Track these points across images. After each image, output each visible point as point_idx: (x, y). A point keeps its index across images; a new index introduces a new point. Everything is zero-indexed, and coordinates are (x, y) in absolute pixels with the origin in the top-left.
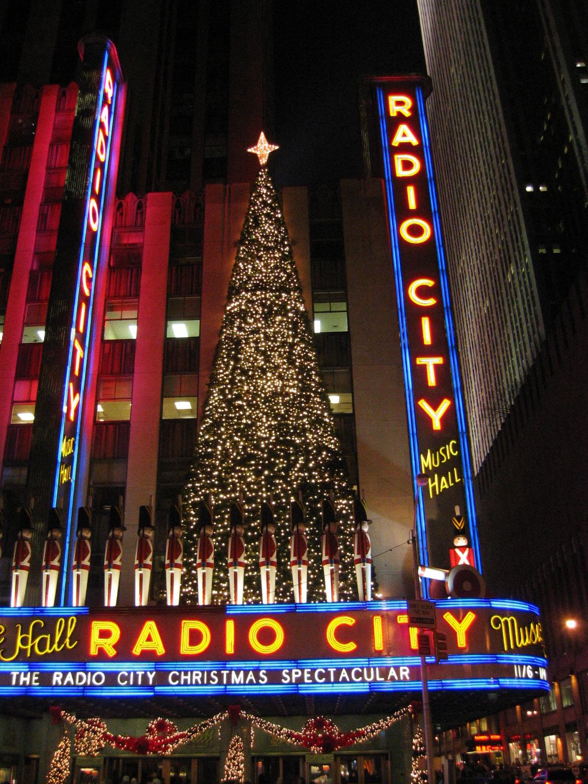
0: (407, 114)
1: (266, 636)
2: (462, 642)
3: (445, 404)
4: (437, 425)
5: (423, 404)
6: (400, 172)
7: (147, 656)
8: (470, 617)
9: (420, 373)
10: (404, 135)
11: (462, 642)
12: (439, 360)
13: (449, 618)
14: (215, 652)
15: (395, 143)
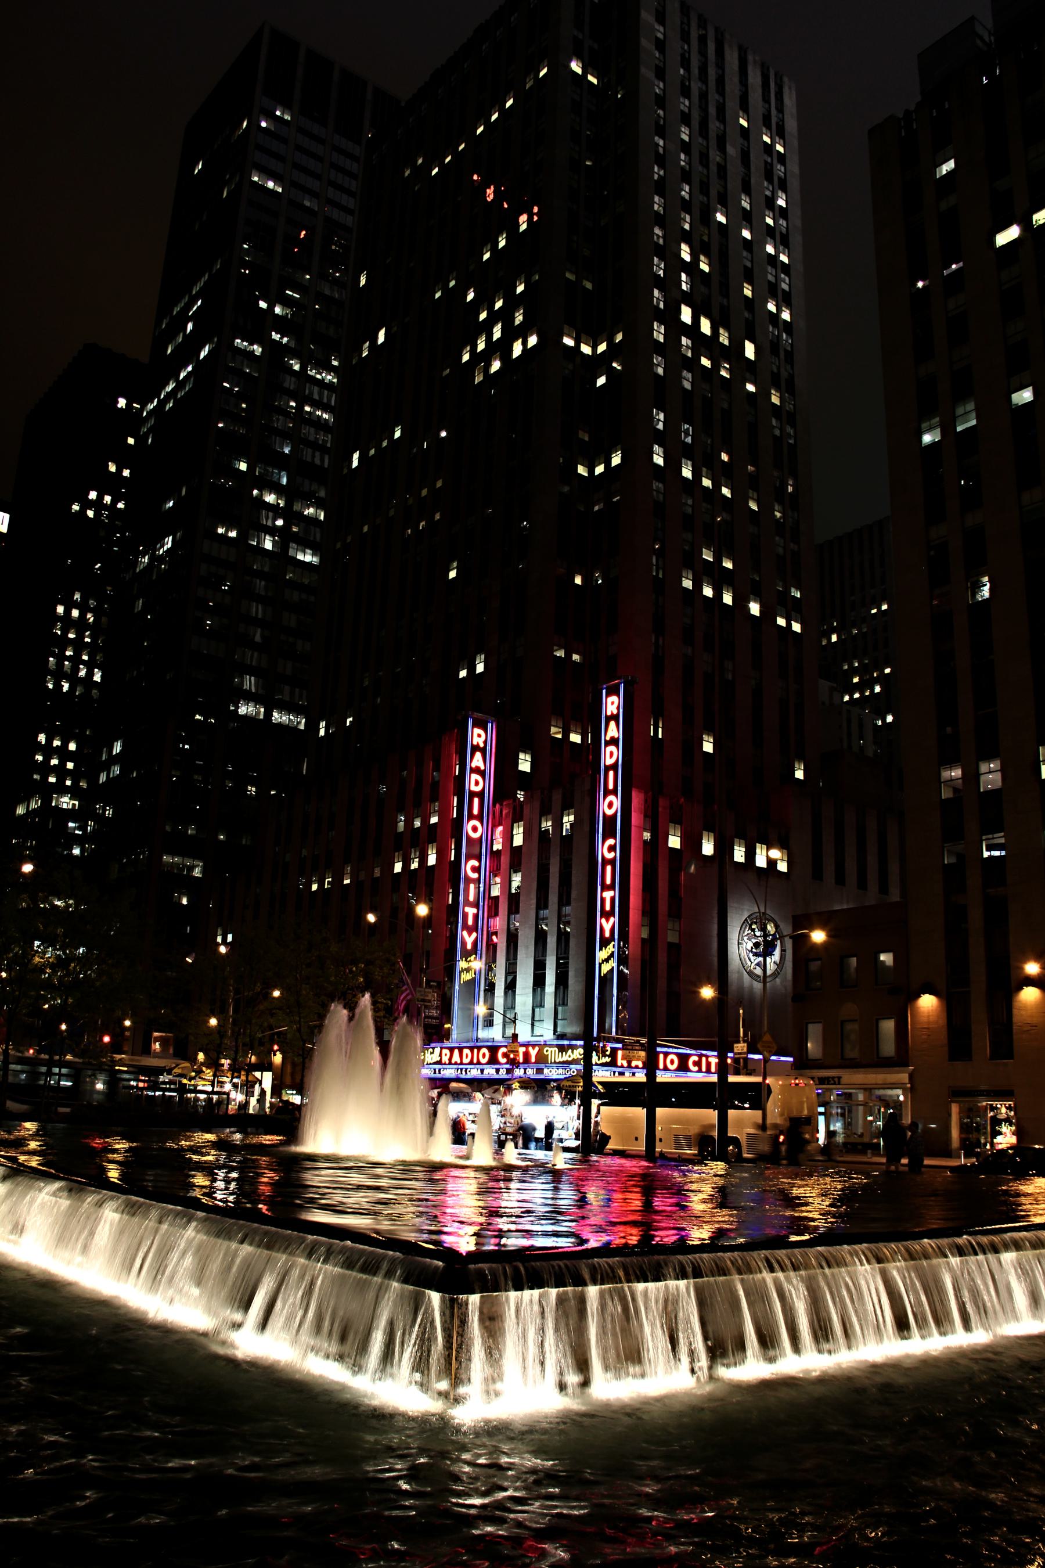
0: (615, 712)
1: (484, 1055)
2: (533, 1060)
3: (612, 920)
4: (607, 934)
5: (603, 921)
6: (610, 761)
7: (456, 1063)
8: (537, 1049)
9: (603, 900)
10: (613, 731)
11: (533, 1060)
12: (611, 893)
13: (530, 1049)
14: (471, 1063)
15: (608, 738)
